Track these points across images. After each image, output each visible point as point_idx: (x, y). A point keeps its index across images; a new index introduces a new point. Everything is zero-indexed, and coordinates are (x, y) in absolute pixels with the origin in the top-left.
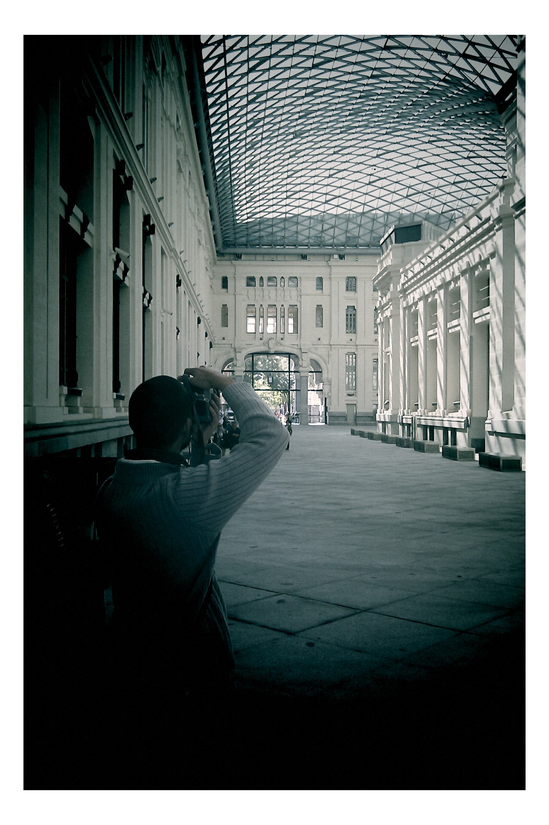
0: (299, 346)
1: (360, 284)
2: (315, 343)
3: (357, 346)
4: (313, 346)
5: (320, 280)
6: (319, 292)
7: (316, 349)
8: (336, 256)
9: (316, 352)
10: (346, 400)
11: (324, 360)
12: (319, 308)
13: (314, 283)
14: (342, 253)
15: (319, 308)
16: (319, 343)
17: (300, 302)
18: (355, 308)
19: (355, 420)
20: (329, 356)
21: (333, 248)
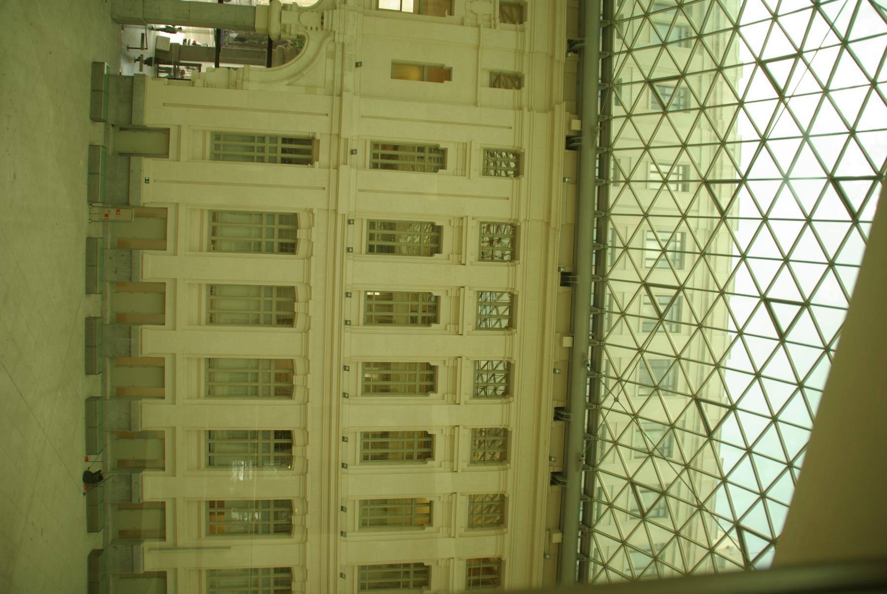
0: (342, 6)
1: (503, 185)
2: (347, 52)
3: (337, 168)
4: (339, 47)
5: (514, 81)
6: (485, 78)
7: (333, 56)
8: (576, 125)
9: (324, 50)
10: (179, 127)
11: (299, 73)
12: (442, 74)
13: (507, 65)
14: (586, 140)
15: (442, 74)
16: (347, 61)
17: (462, 24)
18: (440, 171)
19: (121, 154)
20: (311, 89)
21: (598, 117)
